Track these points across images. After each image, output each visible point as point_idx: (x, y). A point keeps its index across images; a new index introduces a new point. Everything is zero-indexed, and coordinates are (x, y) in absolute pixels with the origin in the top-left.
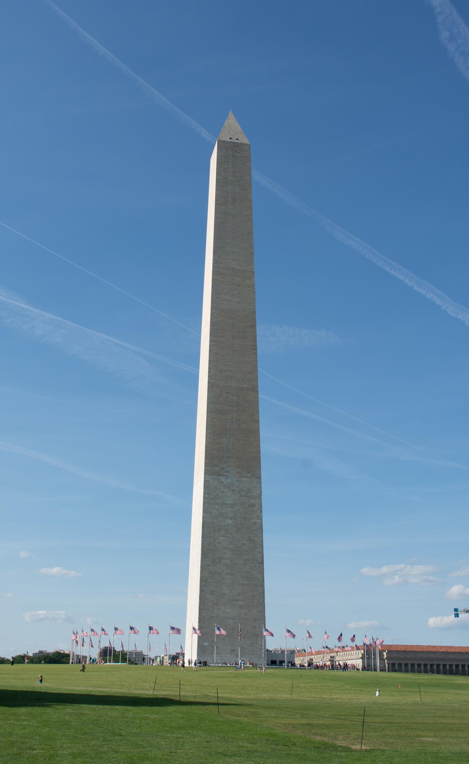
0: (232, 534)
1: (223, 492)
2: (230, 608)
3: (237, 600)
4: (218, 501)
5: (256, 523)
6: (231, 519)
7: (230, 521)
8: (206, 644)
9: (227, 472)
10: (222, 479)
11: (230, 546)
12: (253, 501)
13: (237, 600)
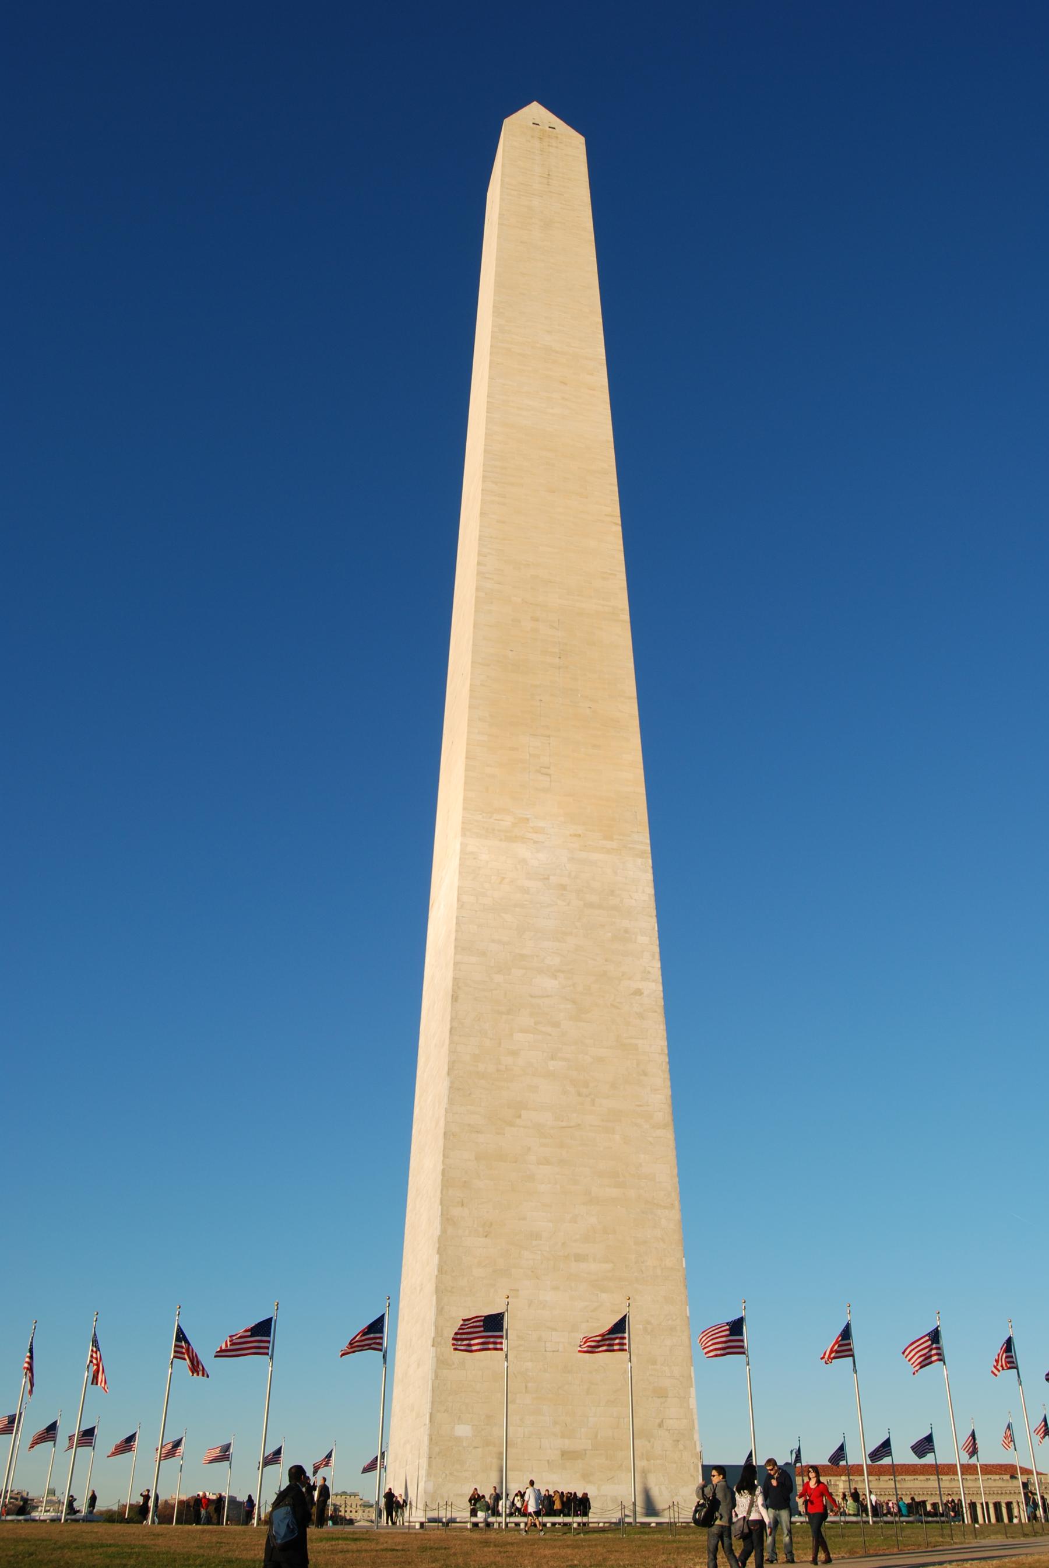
0: (556, 1025)
2: (556, 1288)
3: (579, 1258)
5: (639, 992)
6: (555, 977)
7: (550, 984)
8: (463, 1430)
10: (523, 851)
11: (552, 1065)
13: (579, 1258)
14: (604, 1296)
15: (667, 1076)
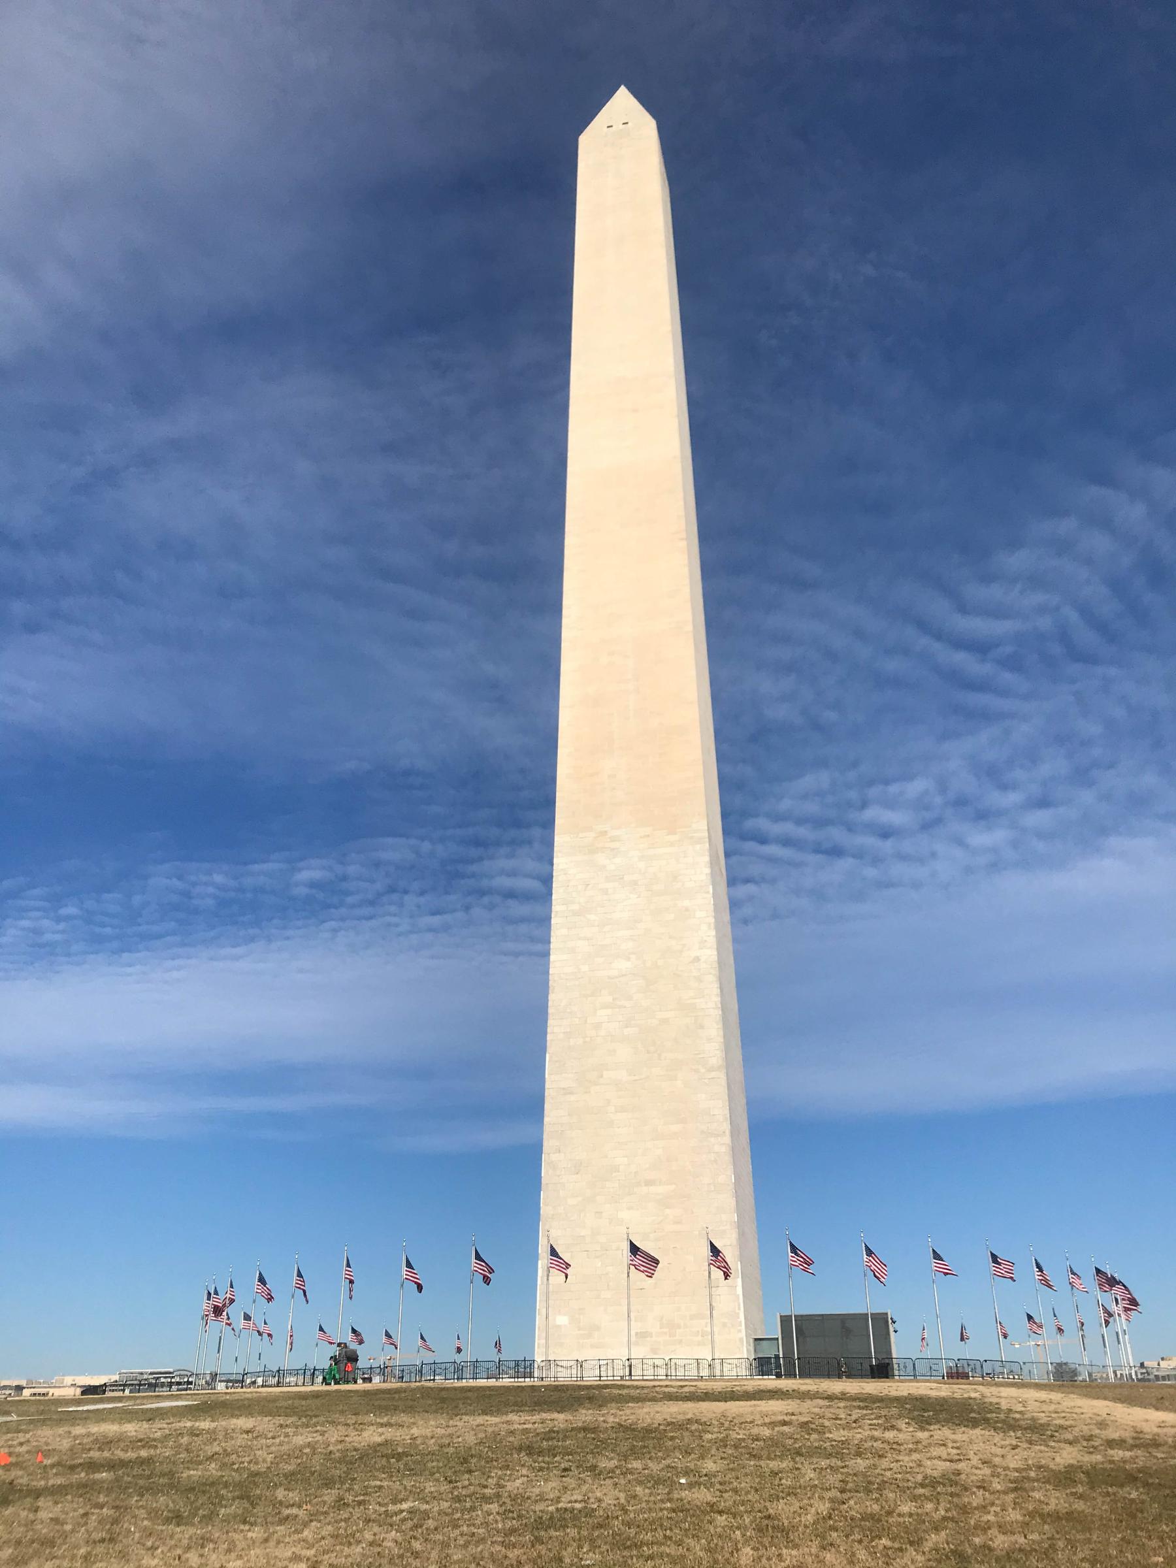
1: (605, 892)
2: (629, 1208)
4: (592, 917)
5: (697, 959)
6: (629, 959)
9: (614, 839)
11: (626, 1031)
12: (687, 903)
13: (649, 1183)
14: (668, 1211)
15: (720, 1026)
